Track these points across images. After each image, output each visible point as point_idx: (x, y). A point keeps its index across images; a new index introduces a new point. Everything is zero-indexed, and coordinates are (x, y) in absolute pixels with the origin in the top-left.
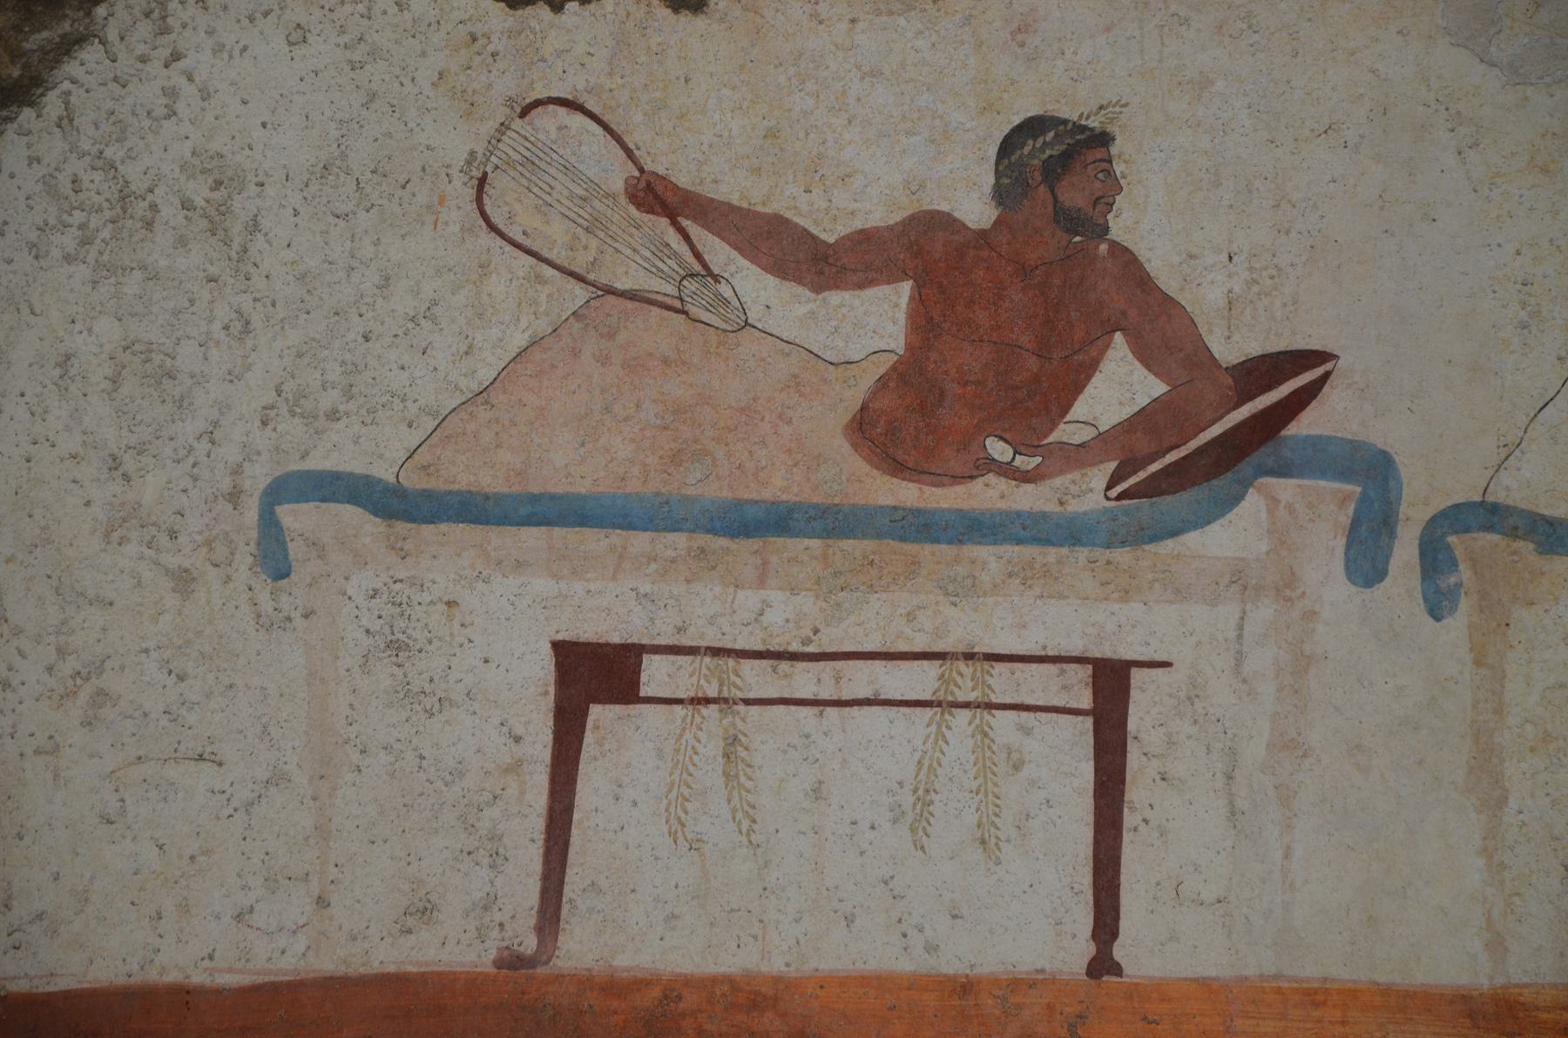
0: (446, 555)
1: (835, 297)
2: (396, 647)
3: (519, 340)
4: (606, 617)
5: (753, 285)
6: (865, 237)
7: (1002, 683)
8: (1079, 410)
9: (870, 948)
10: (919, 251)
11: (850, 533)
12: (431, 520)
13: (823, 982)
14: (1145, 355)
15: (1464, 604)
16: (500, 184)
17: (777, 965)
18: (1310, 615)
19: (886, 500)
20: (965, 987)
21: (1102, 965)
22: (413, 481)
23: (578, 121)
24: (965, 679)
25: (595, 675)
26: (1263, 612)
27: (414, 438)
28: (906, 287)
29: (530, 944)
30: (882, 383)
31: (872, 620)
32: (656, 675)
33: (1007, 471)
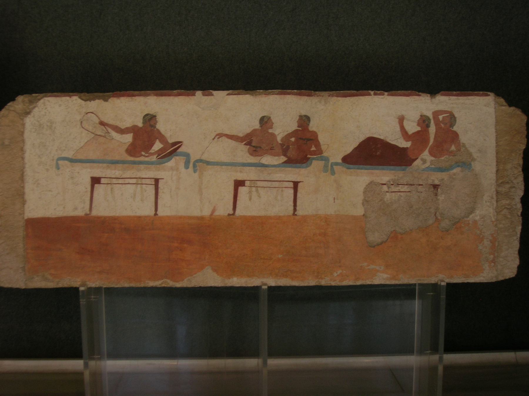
0: (78, 167)
1: (124, 135)
2: (72, 178)
3: (86, 141)
4: (97, 173)
5: (114, 134)
6: (127, 128)
7: (144, 181)
8: (153, 148)
9: (128, 213)
10: (133, 130)
11: (125, 164)
12: (76, 162)
13: (123, 217)
14: (161, 142)
15: (198, 171)
16: (84, 123)
17: (117, 215)
18: (180, 173)
19: (130, 159)
20: (140, 217)
21: (156, 214)
22: (74, 158)
23: (93, 115)
24: (139, 181)
25: (96, 181)
26: (175, 172)
27: (73, 153)
28: (132, 134)
29: (88, 213)
30: (129, 145)
31: (128, 174)
32: (103, 181)
33: (144, 156)
